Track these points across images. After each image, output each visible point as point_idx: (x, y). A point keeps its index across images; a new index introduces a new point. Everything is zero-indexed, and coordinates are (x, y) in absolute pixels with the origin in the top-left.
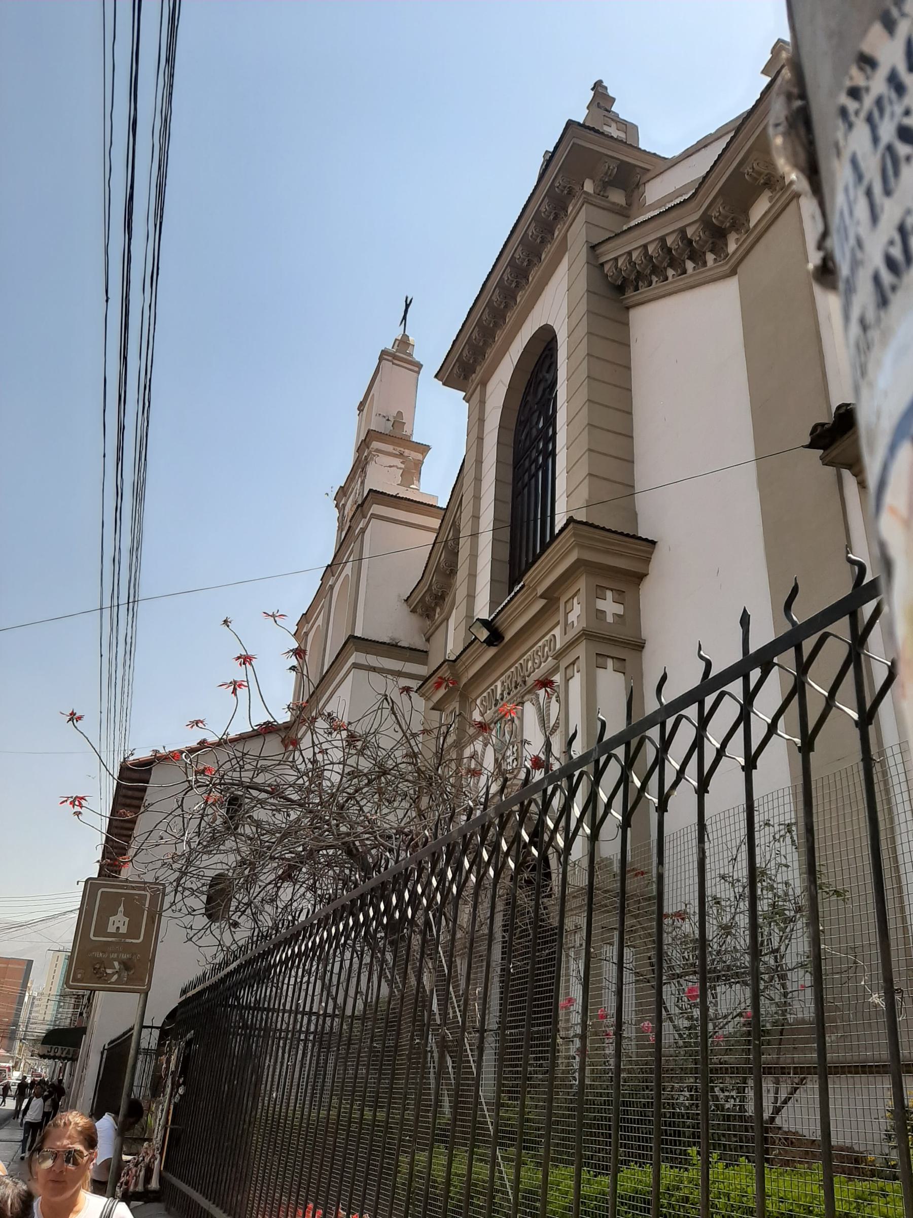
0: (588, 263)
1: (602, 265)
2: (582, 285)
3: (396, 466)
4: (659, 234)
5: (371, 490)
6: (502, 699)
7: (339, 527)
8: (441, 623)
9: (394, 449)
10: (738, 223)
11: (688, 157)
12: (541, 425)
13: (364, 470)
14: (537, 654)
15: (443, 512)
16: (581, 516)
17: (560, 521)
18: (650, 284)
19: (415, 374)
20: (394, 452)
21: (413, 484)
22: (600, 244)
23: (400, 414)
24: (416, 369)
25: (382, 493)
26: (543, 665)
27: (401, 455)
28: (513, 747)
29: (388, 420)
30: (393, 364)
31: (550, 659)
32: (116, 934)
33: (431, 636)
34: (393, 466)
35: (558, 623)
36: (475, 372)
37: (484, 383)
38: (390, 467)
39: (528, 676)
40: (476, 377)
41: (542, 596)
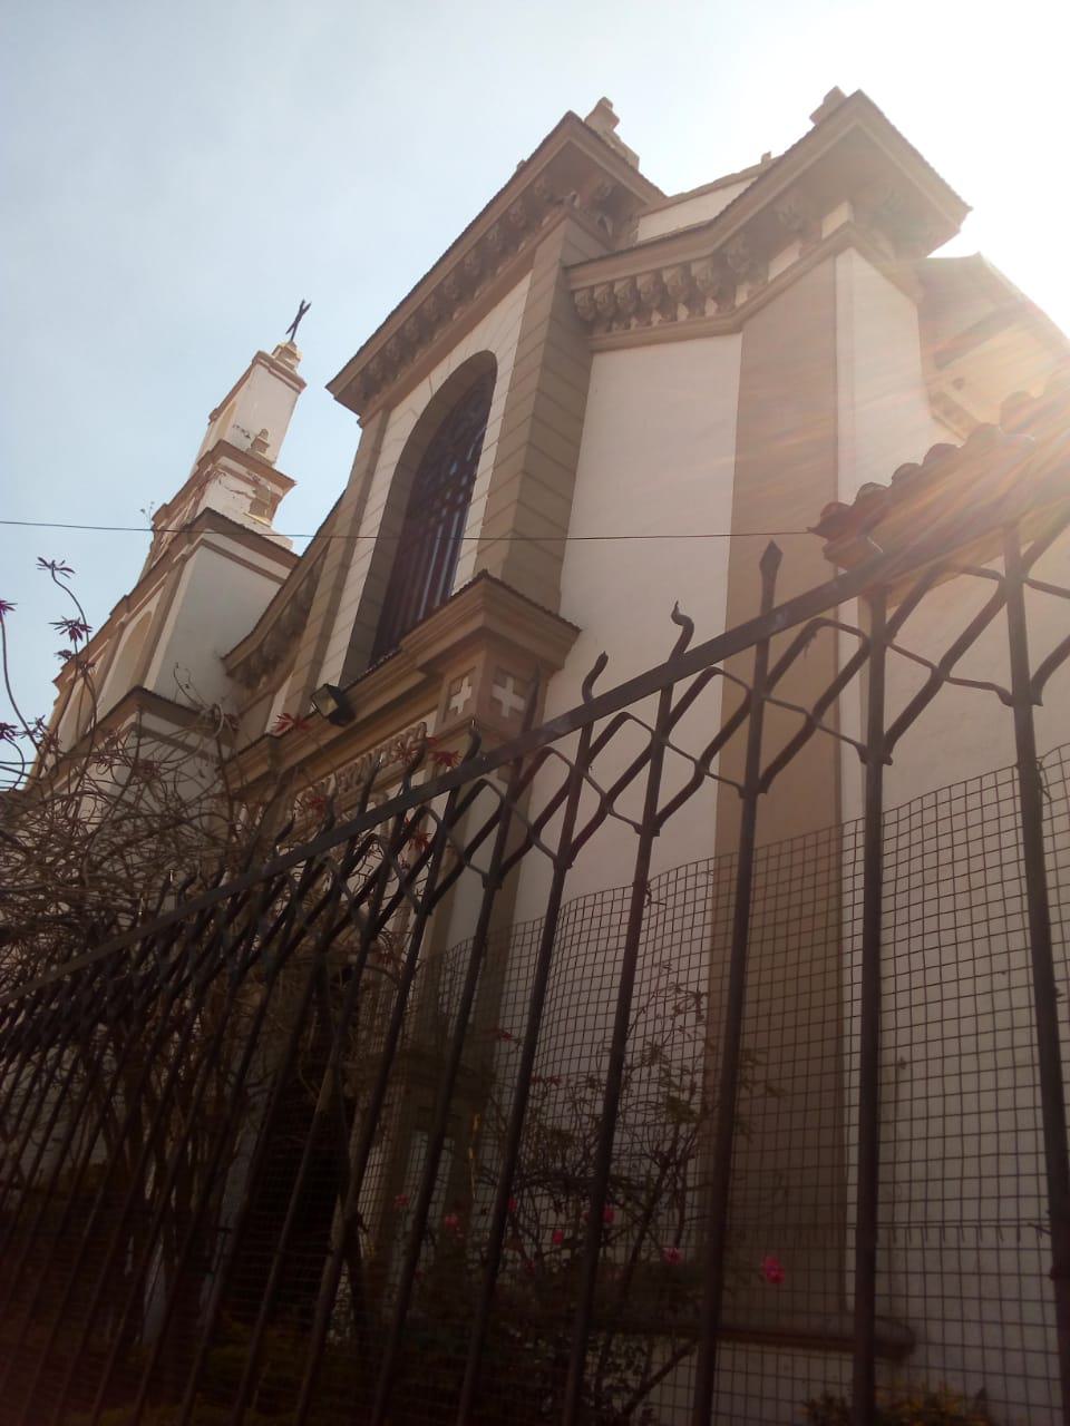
2: (545, 307)
5: (208, 510)
8: (265, 695)
12: (453, 470)
16: (497, 574)
17: (464, 573)
23: (264, 432)
24: (297, 387)
29: (248, 437)
30: (270, 371)
33: (249, 709)
34: (242, 493)
35: (435, 708)
36: (378, 393)
37: (389, 408)
38: (238, 493)
40: (379, 399)
41: (422, 669)
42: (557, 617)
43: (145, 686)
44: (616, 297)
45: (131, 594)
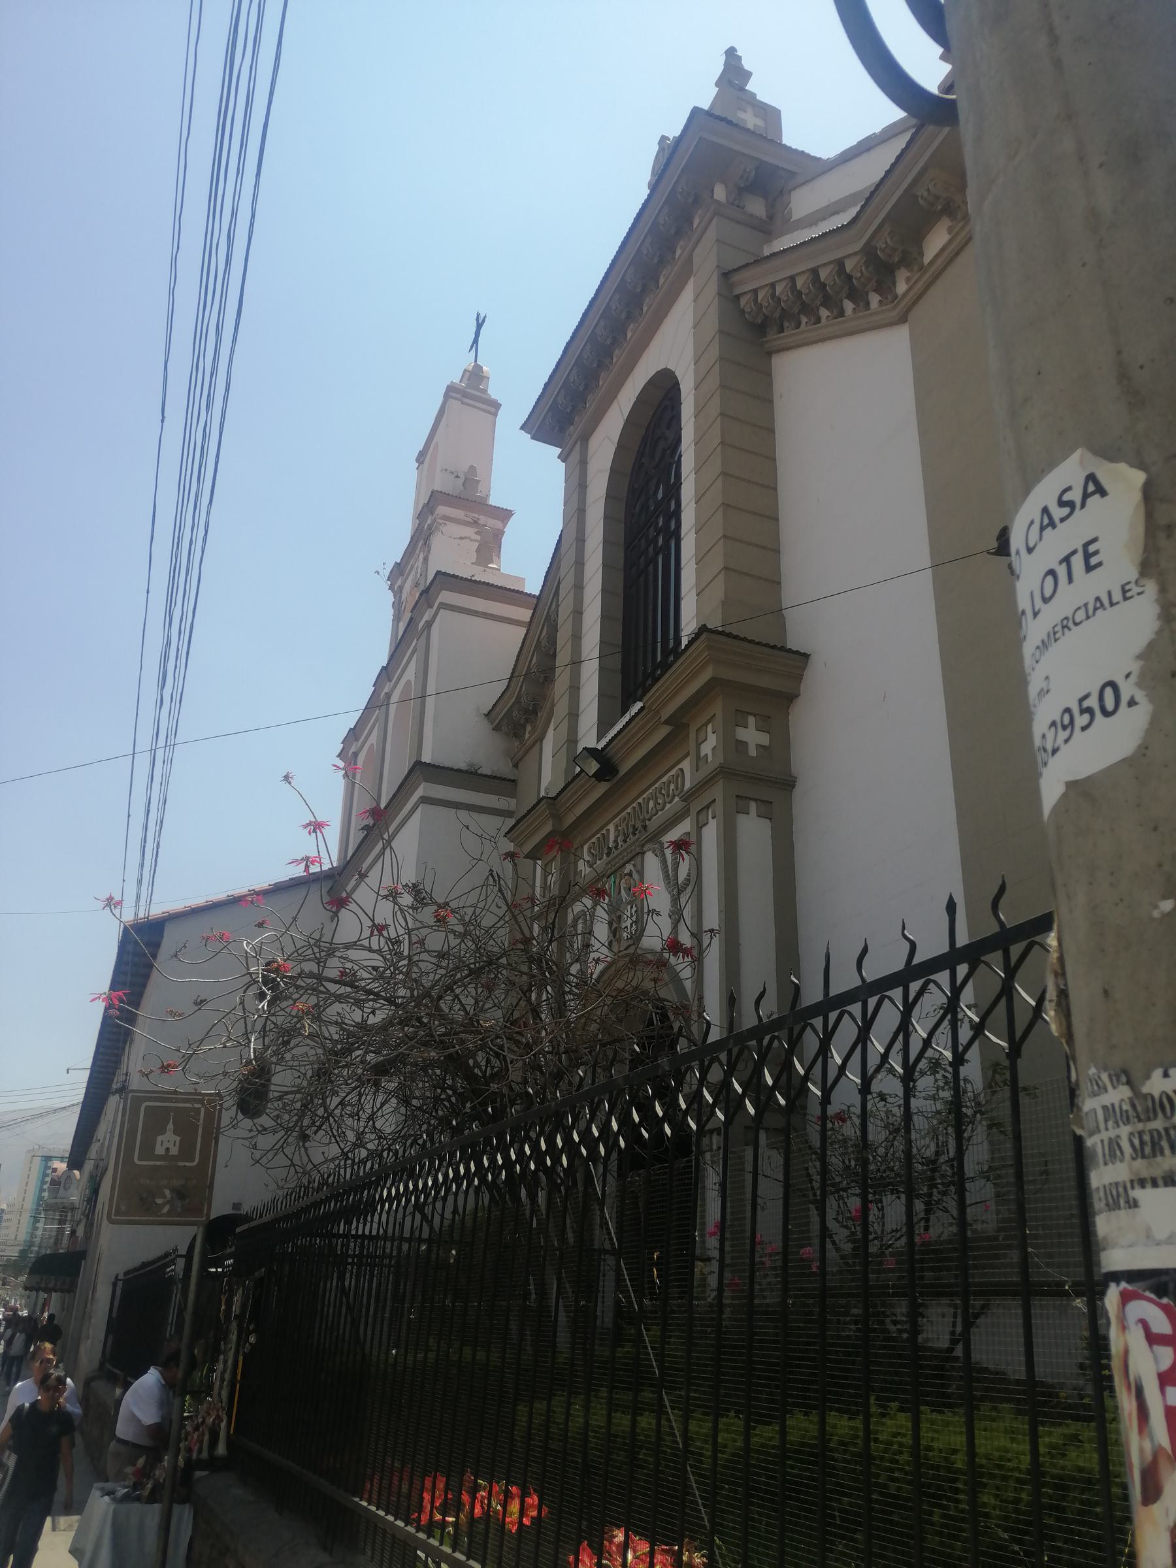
0: (719, 294)
1: (738, 297)
2: (712, 322)
3: (469, 538)
4: (811, 265)
5: (438, 573)
6: (616, 848)
7: (394, 615)
10: (909, 257)
11: (846, 161)
12: (660, 495)
13: (426, 541)
14: (660, 793)
15: (535, 601)
16: (715, 623)
17: (689, 626)
18: (798, 326)
20: (466, 519)
21: (492, 562)
22: (735, 270)
24: (493, 410)
25: (454, 576)
26: (668, 806)
27: (475, 523)
28: (632, 907)
29: (457, 477)
31: (677, 799)
32: (166, 1156)
33: (521, 759)
36: (573, 424)
38: (461, 538)
39: (649, 820)
40: (574, 431)
41: (667, 722)
42: (783, 649)
45: (388, 664)
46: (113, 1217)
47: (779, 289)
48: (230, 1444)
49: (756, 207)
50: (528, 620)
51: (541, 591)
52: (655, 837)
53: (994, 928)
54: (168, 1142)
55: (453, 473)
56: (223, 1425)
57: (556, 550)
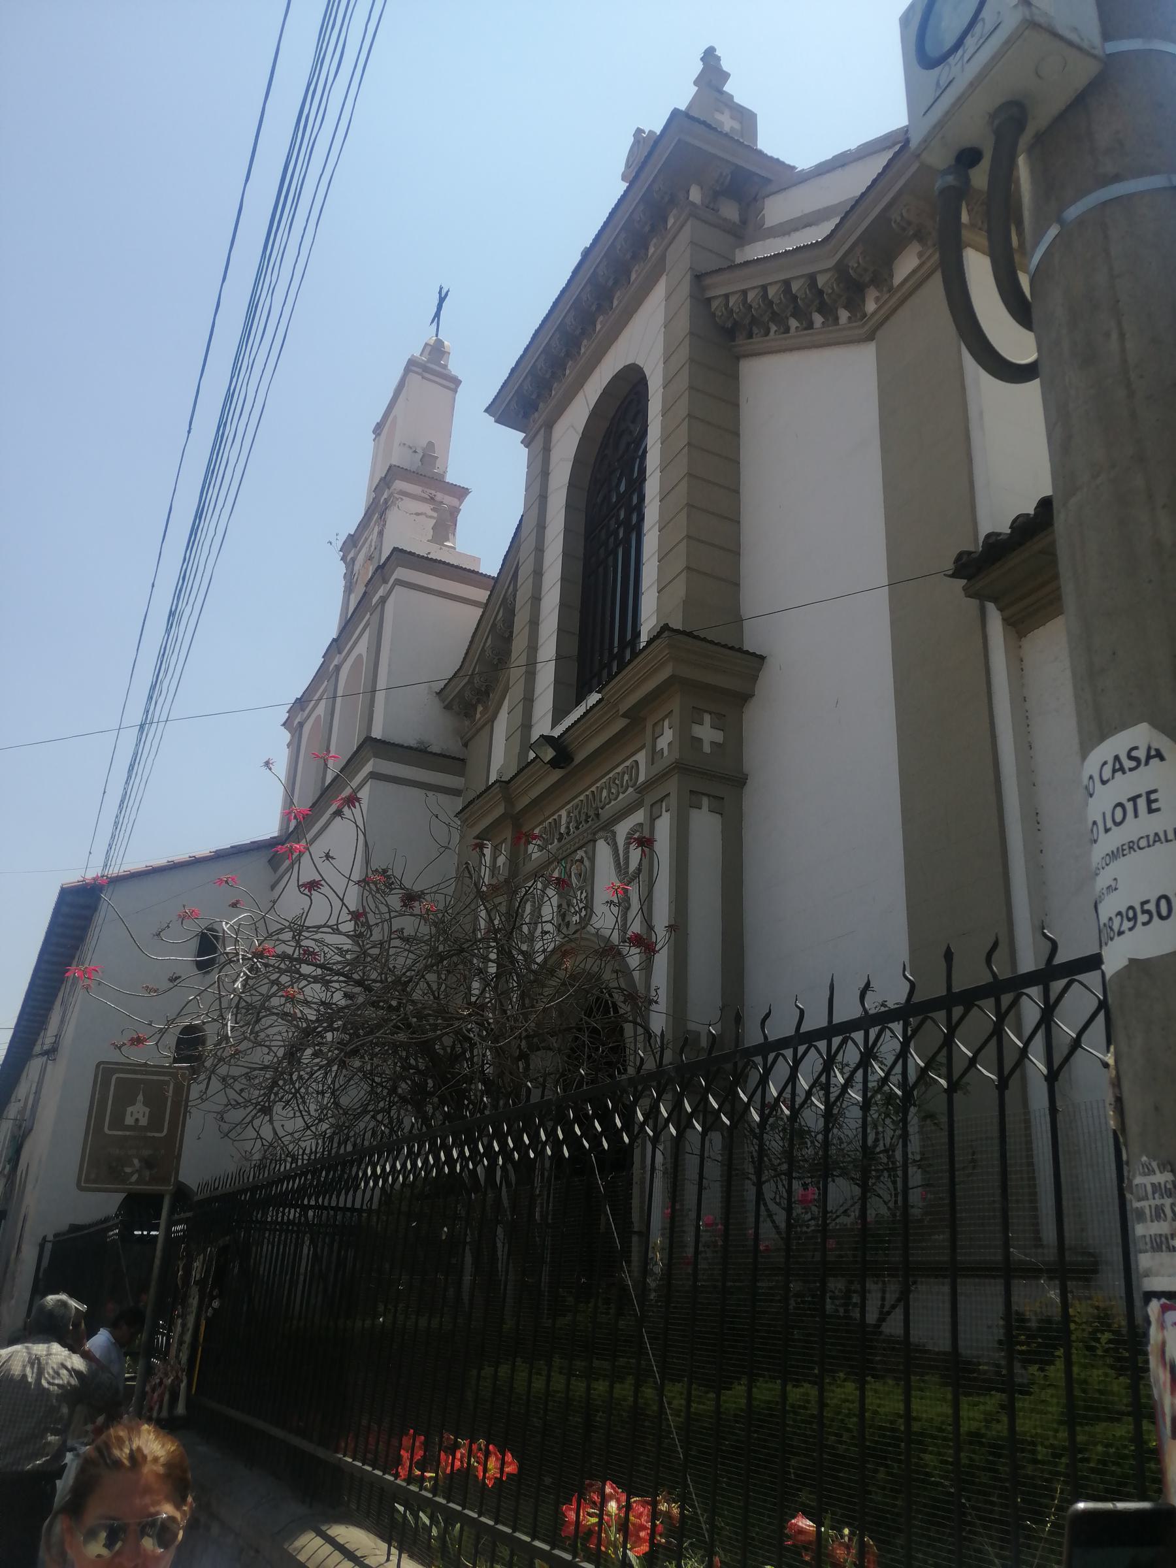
0: (692, 296)
1: (709, 300)
2: (683, 323)
5: (395, 549)
6: (568, 834)
7: (345, 587)
8: (485, 724)
9: (423, 491)
10: (880, 277)
11: (820, 175)
12: (622, 488)
13: (382, 515)
14: (614, 782)
15: (492, 582)
16: (677, 624)
17: (648, 624)
18: (767, 333)
19: (450, 393)
20: (423, 495)
21: (448, 540)
22: (707, 274)
23: (431, 445)
24: (452, 386)
25: (410, 553)
26: (621, 796)
27: (432, 499)
28: (582, 893)
29: (415, 452)
30: (423, 378)
31: (630, 790)
32: (136, 1127)
33: (470, 740)
36: (537, 410)
38: (418, 514)
39: (602, 809)
41: (624, 715)
42: (740, 650)
43: (374, 735)
44: (751, 307)
45: (339, 636)
46: (83, 1184)
47: (751, 296)
48: (189, 1405)
49: (730, 211)
50: (485, 601)
51: (499, 574)
52: (607, 828)
53: (987, 978)
54: (138, 1113)
55: (410, 447)
56: (183, 1385)
57: (515, 534)
